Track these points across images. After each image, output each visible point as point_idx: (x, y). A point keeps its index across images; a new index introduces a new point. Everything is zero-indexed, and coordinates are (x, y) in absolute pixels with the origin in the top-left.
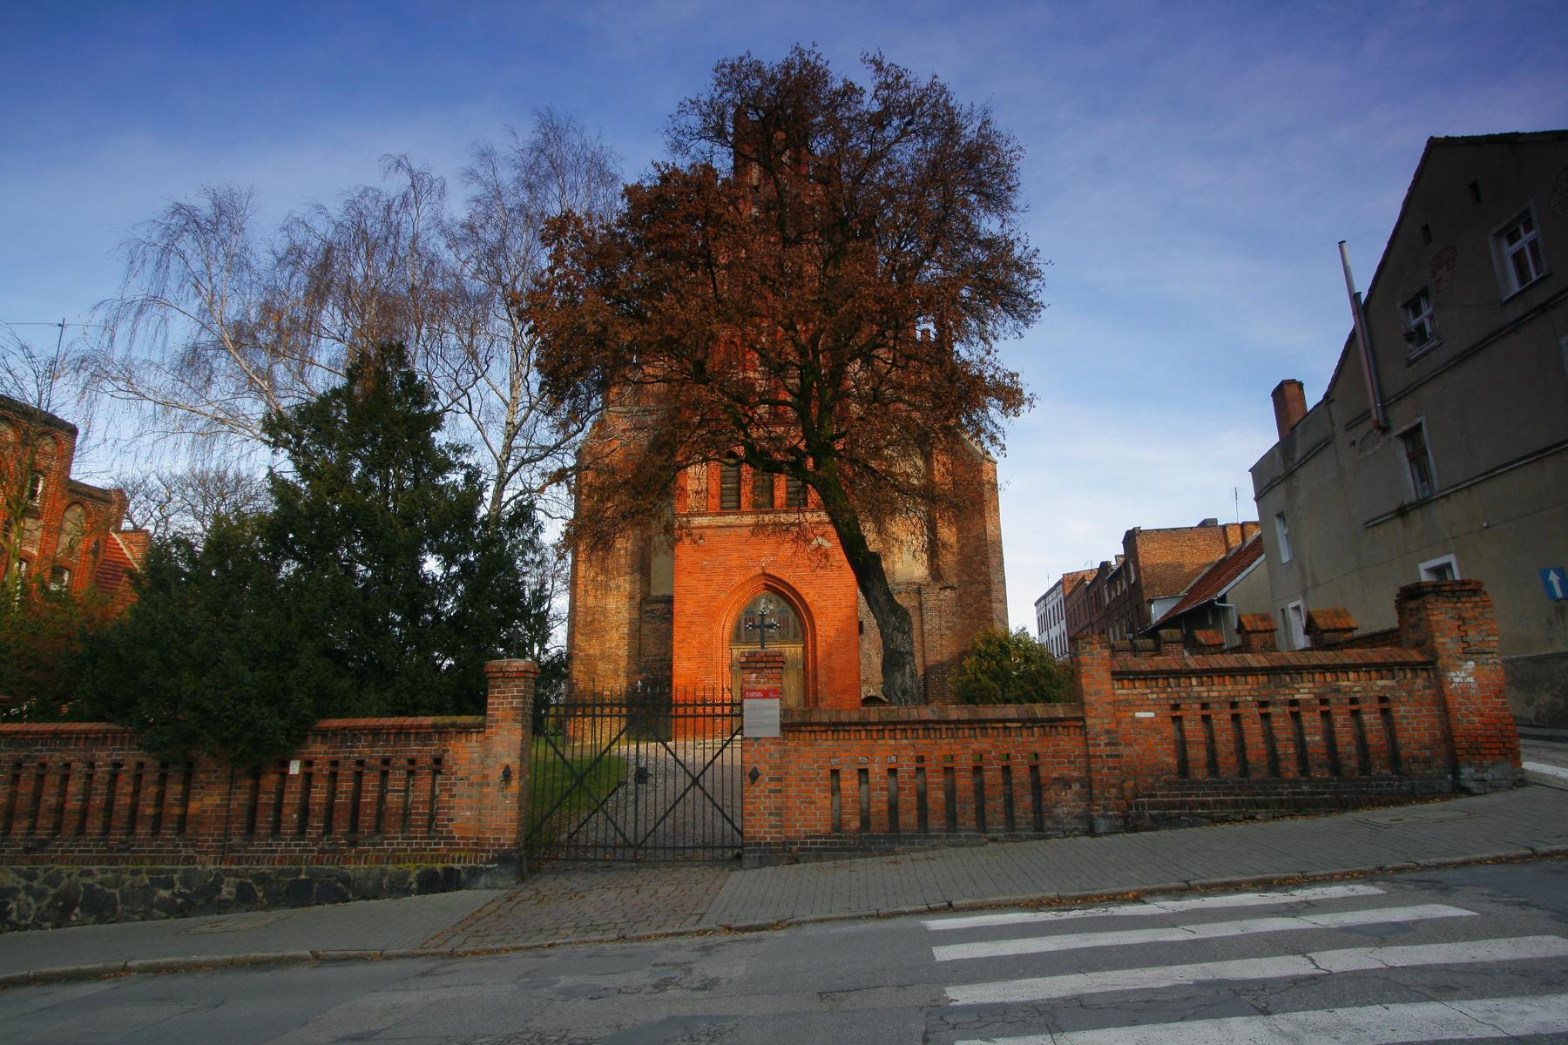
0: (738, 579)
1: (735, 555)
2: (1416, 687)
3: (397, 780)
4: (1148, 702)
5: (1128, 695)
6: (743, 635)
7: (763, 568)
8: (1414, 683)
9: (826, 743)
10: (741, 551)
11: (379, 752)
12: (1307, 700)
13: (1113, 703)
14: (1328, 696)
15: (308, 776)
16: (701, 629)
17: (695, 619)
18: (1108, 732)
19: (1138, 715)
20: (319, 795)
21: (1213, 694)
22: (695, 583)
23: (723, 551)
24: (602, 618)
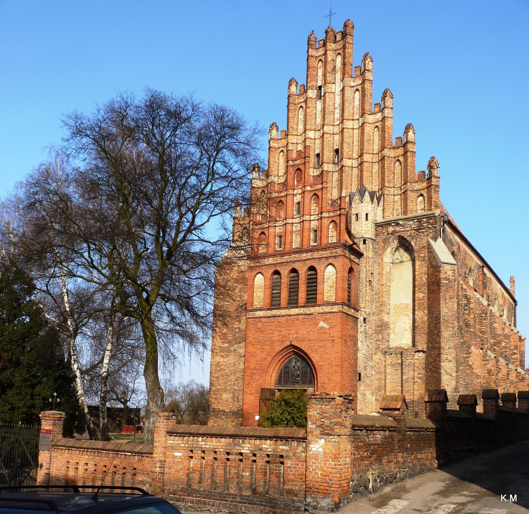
0: (278, 348)
1: (276, 334)
2: (297, 451)
4: (180, 448)
5: (173, 444)
6: (283, 381)
7: (291, 341)
8: (297, 449)
10: (280, 331)
12: (247, 454)
13: (165, 448)
14: (256, 452)
16: (257, 378)
17: (255, 371)
18: (161, 461)
19: (176, 454)
21: (207, 446)
22: (255, 350)
23: (270, 332)
24: (225, 368)
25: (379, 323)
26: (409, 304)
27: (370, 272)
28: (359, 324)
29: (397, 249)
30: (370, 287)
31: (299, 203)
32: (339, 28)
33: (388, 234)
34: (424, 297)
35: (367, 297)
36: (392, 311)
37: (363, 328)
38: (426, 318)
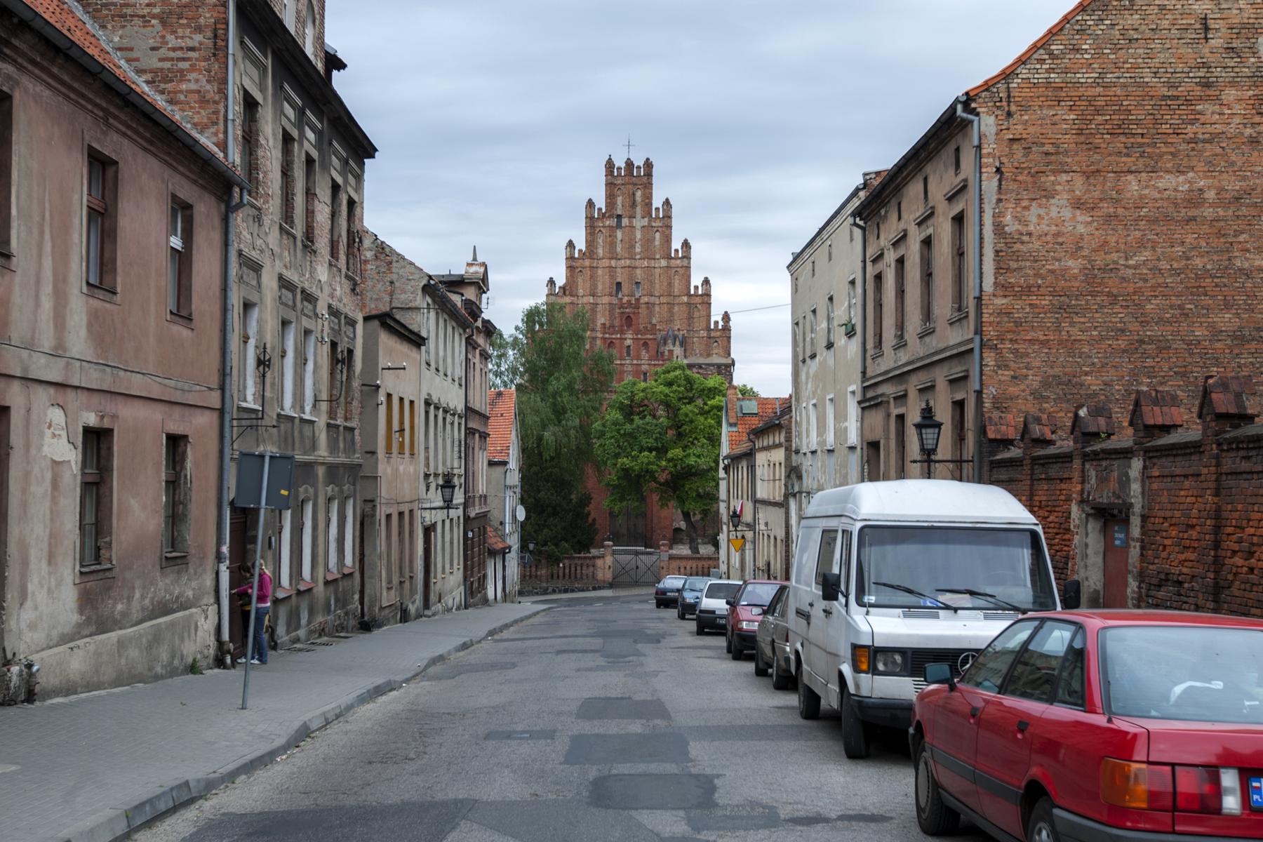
3: (585, 568)
9: (678, 562)
11: (579, 562)
15: (564, 567)
20: (567, 571)
31: (629, 347)
32: (639, 161)
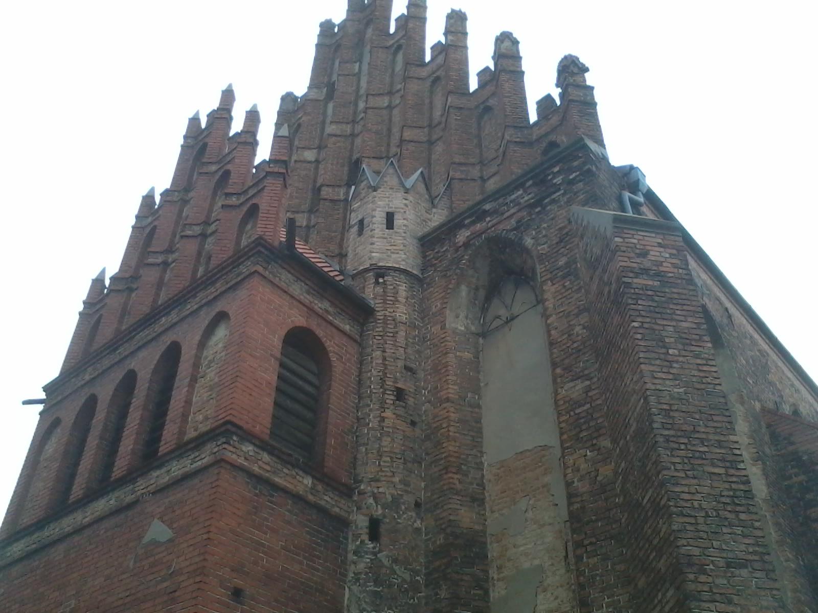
25: (441, 540)
26: (545, 447)
27: (400, 364)
28: (351, 547)
29: (493, 291)
30: (401, 411)
33: (457, 250)
34: (588, 390)
35: (386, 441)
36: (492, 491)
37: (367, 559)
38: (606, 471)
